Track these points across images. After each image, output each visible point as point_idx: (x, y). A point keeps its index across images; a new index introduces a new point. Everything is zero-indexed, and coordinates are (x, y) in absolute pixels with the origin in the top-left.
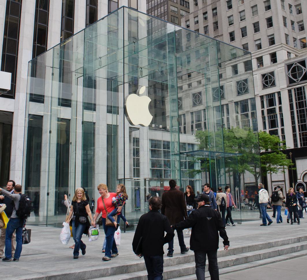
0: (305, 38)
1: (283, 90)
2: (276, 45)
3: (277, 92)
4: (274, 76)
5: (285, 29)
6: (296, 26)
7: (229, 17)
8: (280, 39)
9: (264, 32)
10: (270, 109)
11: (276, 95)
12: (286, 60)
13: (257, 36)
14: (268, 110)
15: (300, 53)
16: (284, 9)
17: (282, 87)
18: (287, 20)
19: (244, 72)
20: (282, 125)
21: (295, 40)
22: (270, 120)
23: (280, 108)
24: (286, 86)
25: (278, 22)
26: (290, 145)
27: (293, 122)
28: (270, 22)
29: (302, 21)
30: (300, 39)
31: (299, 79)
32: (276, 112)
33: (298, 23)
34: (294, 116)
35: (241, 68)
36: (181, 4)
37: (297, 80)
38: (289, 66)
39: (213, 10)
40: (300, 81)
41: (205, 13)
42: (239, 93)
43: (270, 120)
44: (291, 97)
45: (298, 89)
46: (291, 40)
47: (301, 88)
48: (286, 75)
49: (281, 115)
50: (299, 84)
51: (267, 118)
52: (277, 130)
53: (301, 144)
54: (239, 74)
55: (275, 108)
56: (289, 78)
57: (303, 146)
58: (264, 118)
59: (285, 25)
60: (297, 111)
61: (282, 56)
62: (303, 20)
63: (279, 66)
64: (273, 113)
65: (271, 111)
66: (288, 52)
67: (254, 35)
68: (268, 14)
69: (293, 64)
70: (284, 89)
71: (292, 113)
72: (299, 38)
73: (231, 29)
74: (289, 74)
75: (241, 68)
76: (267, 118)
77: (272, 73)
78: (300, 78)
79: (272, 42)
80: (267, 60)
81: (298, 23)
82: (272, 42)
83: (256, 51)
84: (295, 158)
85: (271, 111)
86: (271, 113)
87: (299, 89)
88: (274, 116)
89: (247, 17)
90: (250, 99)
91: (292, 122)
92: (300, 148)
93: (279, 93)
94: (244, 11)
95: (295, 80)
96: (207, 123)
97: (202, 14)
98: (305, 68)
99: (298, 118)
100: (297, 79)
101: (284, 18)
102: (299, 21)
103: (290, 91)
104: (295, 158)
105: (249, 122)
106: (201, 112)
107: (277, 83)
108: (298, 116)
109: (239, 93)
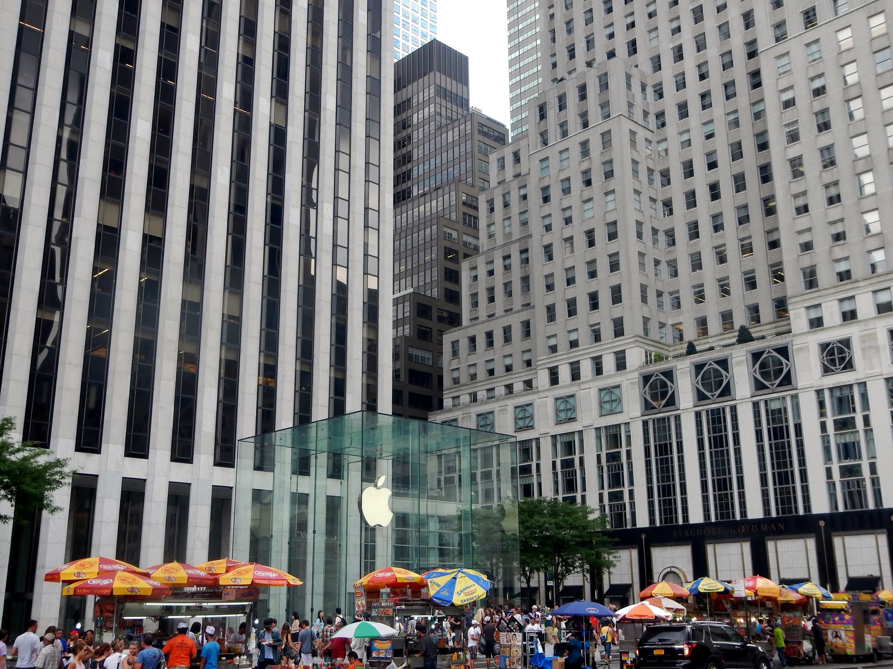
0: (681, 323)
1: (634, 420)
2: (626, 337)
5: (644, 307)
6: (667, 300)
7: (547, 277)
8: (633, 326)
9: (607, 312)
11: (623, 428)
13: (595, 317)
14: (607, 454)
15: (671, 349)
17: (632, 415)
19: (569, 382)
20: (631, 483)
21: (662, 325)
23: (629, 453)
24: (639, 414)
25: (630, 294)
27: (649, 480)
28: (616, 295)
29: (678, 292)
30: (673, 325)
31: (715, 393)
33: (671, 294)
34: (650, 469)
35: (564, 373)
36: (465, 223)
37: (713, 396)
38: (646, 378)
39: (522, 252)
40: (718, 397)
41: (507, 257)
44: (648, 434)
45: (659, 419)
46: (653, 326)
47: (664, 419)
49: (630, 465)
51: (605, 469)
52: (622, 492)
53: (661, 519)
55: (619, 452)
57: (663, 524)
58: (600, 468)
60: (657, 460)
61: (635, 357)
62: (679, 290)
63: (630, 376)
64: (617, 461)
67: (589, 316)
68: (615, 280)
69: (653, 375)
70: (636, 419)
71: (648, 463)
72: (670, 322)
73: (549, 301)
75: (564, 373)
76: (605, 469)
78: (778, 381)
79: (619, 331)
80: (609, 363)
81: (671, 294)
82: (619, 331)
83: (592, 346)
86: (613, 461)
88: (619, 466)
90: (561, 435)
91: (648, 479)
94: (573, 267)
97: (502, 259)
100: (712, 394)
101: (644, 289)
102: (671, 290)
103: (645, 423)
108: (657, 469)
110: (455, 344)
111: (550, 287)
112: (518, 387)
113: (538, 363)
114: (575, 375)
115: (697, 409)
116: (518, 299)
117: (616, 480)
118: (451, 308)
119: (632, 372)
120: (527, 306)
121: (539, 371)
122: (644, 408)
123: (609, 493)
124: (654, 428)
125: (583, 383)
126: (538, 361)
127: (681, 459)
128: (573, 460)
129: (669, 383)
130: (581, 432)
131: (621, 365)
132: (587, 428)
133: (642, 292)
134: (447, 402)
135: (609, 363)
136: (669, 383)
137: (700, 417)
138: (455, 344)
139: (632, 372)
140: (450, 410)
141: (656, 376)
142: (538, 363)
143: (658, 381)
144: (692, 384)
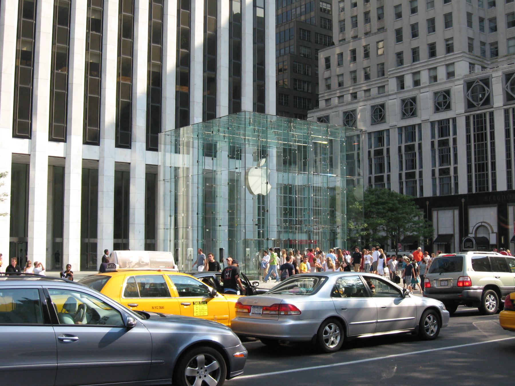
1: (459, 115)
2: (455, 53)
3: (452, 118)
4: (415, 103)
10: (378, 150)
12: (466, 76)
14: (439, 141)
16: (470, 2)
17: (458, 112)
18: (473, 16)
22: (441, 154)
23: (455, 140)
26: (428, 193)
27: (469, 160)
32: (449, 145)
38: (469, 85)
42: (437, 110)
43: (441, 154)
46: (477, 45)
47: (481, 115)
48: (465, 97)
49: (455, 149)
50: (480, 109)
52: (449, 169)
54: (421, 86)
55: (448, 140)
56: (507, 93)
59: (470, 24)
60: (475, 145)
63: (457, 83)
65: (444, 143)
66: (470, 63)
70: (461, 115)
71: (469, 148)
73: (398, 26)
74: (468, 94)
75: (409, 81)
77: (414, 99)
82: (449, 49)
84: (432, 209)
85: (444, 143)
87: (479, 116)
89: (420, 9)
92: (419, 198)
93: (454, 119)
95: (475, 103)
96: (361, 154)
98: (488, 89)
99: (475, 155)
101: (469, 15)
103: (468, 118)
104: (432, 209)
105: (450, 152)
106: (384, 134)
107: (453, 105)
109: (437, 110)
110: (327, 60)
111: (399, 15)
112: (374, 91)
113: (389, 73)
114: (417, 83)
115: (505, 107)
116: (375, 24)
117: (444, 159)
118: (325, 32)
119: (459, 80)
120: (382, 29)
121: (389, 80)
122: (467, 107)
123: (440, 170)
124: (474, 122)
125: (422, 88)
126: (389, 71)
127: (493, 144)
128: (413, 146)
129: (486, 88)
130: (420, 125)
131: (450, 75)
132: (424, 122)
133: (468, 18)
134: (322, 104)
135: (441, 73)
136: (486, 88)
137: (508, 113)
138: (327, 60)
139: (459, 80)
140: (323, 110)
141: (476, 83)
142: (389, 73)
143: (478, 86)
144: (503, 89)
